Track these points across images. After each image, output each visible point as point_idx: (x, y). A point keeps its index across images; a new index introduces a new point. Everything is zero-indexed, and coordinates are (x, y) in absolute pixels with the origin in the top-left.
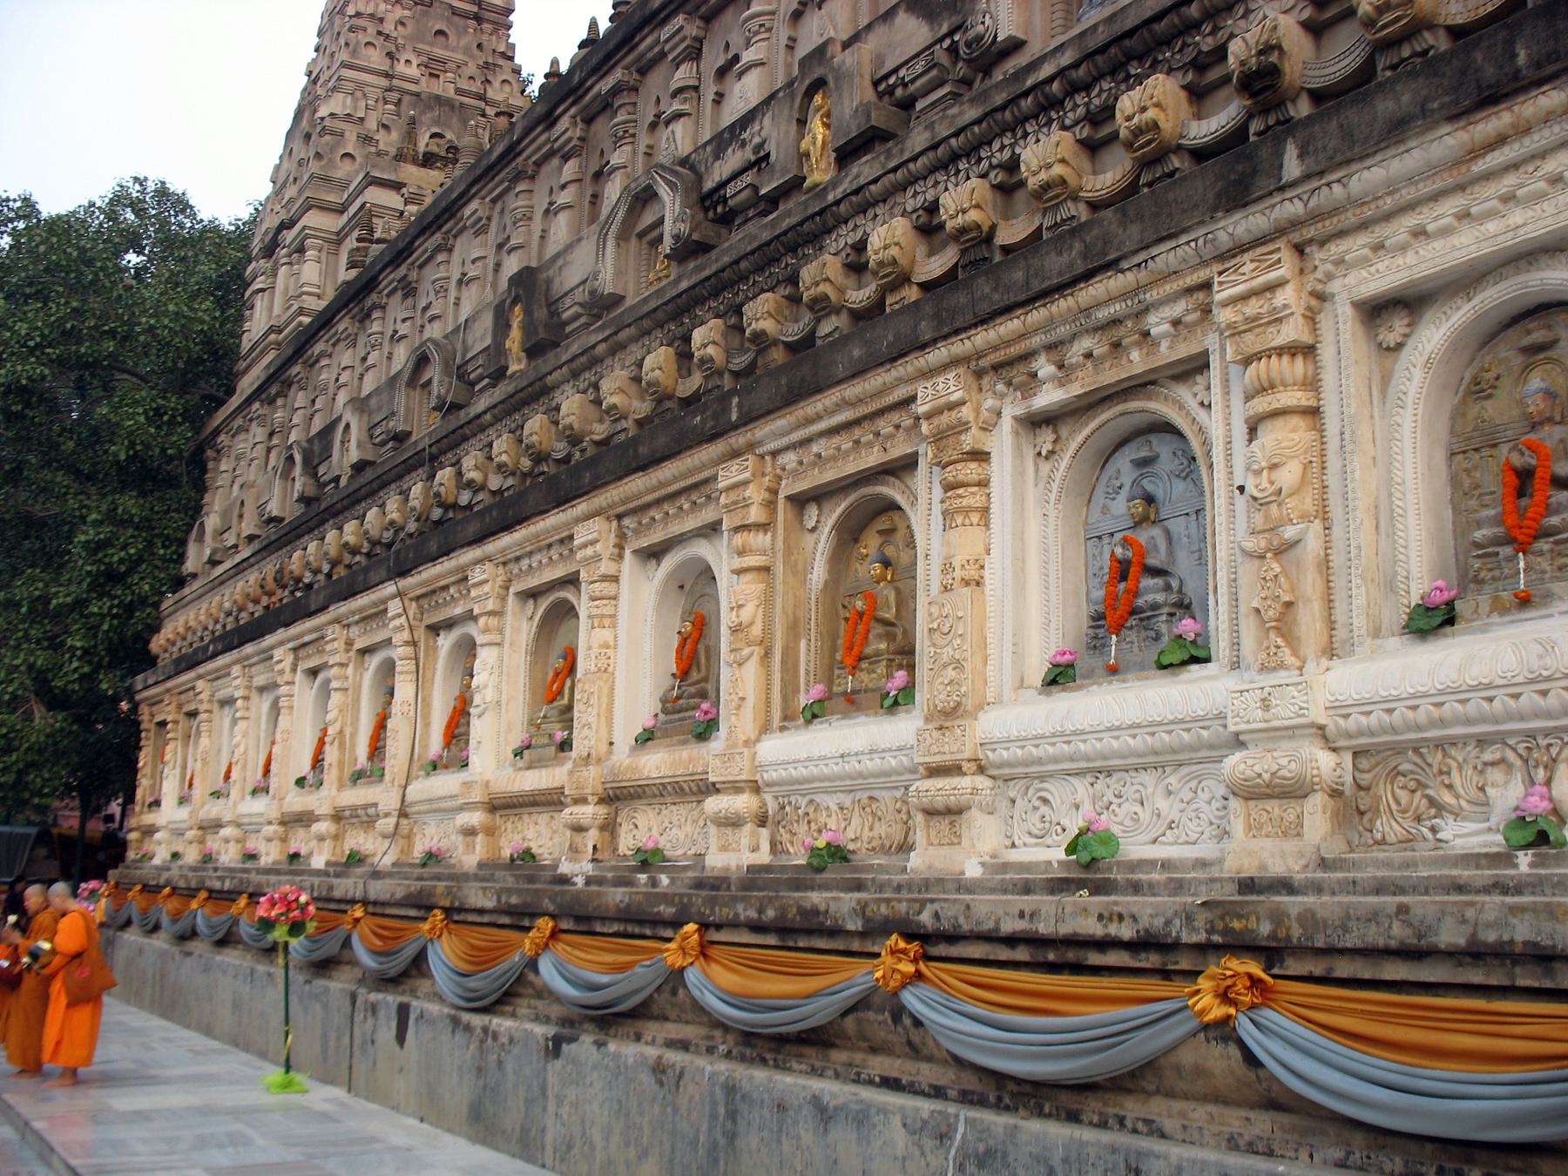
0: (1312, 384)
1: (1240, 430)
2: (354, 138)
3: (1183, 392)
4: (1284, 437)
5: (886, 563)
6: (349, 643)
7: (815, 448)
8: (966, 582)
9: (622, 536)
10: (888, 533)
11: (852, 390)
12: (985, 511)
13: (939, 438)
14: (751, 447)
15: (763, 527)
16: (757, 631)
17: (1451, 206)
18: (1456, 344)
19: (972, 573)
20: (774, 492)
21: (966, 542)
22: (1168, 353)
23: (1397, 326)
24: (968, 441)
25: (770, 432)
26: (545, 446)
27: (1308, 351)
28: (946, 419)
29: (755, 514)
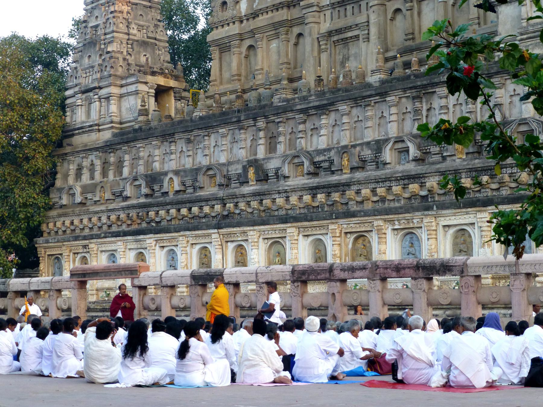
0: (436, 235)
1: (426, 239)
2: (122, 60)
3: (418, 230)
4: (432, 241)
5: (364, 246)
6: (188, 242)
7: (351, 225)
8: (383, 253)
9: (299, 231)
10: (364, 240)
11: (360, 219)
12: (386, 242)
13: (378, 230)
14: (337, 222)
15: (339, 237)
16: (338, 255)
17: (454, 217)
18: (454, 233)
19: (384, 252)
20: (341, 231)
21: (383, 247)
22: (416, 225)
23: (447, 229)
24: (383, 231)
25: (341, 221)
26: (270, 207)
27: (436, 230)
28: (379, 227)
29: (338, 235)
